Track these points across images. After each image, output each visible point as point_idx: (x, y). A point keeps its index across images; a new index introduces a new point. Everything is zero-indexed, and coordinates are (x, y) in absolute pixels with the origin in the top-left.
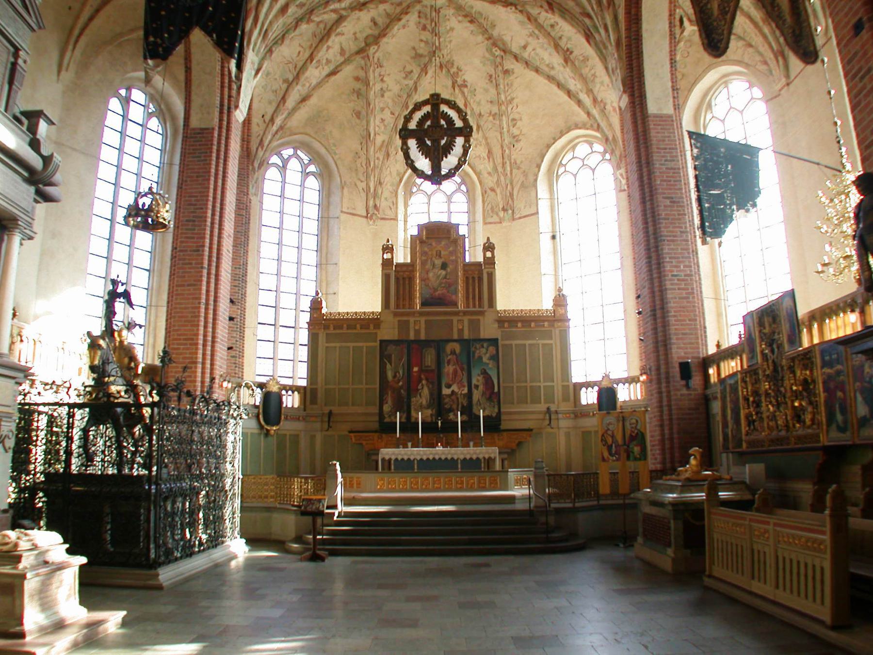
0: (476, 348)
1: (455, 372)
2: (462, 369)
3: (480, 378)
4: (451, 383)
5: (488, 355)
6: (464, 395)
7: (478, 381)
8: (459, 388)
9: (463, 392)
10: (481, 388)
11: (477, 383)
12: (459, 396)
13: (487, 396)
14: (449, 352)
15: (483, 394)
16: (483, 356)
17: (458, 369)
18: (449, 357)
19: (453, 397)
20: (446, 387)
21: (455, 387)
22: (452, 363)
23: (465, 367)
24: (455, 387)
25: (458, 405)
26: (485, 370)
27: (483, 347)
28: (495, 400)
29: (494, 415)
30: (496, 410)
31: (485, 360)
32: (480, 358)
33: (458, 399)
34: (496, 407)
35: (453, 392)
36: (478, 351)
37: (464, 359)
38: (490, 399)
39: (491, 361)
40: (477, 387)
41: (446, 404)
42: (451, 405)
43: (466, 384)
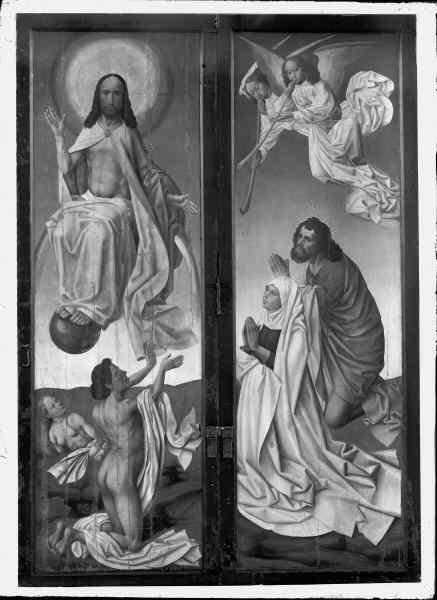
0: (262, 77)
1: (124, 238)
2: (170, 222)
3: (291, 286)
4: (90, 311)
5: (343, 130)
6: (180, 393)
7: (275, 304)
8: (149, 351)
9: (173, 378)
10: (294, 351)
11: (262, 319)
12: (143, 401)
13: (335, 409)
14: (81, 102)
15: (310, 388)
16: (311, 132)
17: (142, 215)
18: (86, 138)
19: (110, 411)
20: (57, 339)
21: (117, 346)
22: (102, 175)
23: (192, 204)
24: (117, 346)
25: (137, 470)
26: (322, 231)
27: (314, 78)
28: (387, 436)
29: (376, 533)
30: (392, 501)
31: (320, 160)
32: (293, 145)
33: (136, 418)
34: (394, 476)
35: (104, 373)
36: (275, 104)
37: (191, 153)
38: (349, 425)
39: (365, 171)
40: (266, 342)
41: (55, 457)
42: (93, 465)
43: (192, 323)
